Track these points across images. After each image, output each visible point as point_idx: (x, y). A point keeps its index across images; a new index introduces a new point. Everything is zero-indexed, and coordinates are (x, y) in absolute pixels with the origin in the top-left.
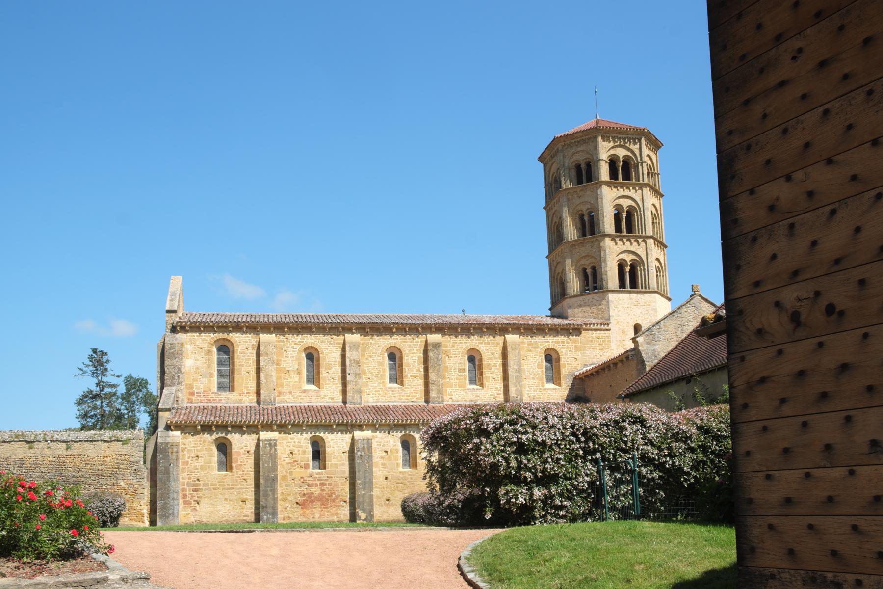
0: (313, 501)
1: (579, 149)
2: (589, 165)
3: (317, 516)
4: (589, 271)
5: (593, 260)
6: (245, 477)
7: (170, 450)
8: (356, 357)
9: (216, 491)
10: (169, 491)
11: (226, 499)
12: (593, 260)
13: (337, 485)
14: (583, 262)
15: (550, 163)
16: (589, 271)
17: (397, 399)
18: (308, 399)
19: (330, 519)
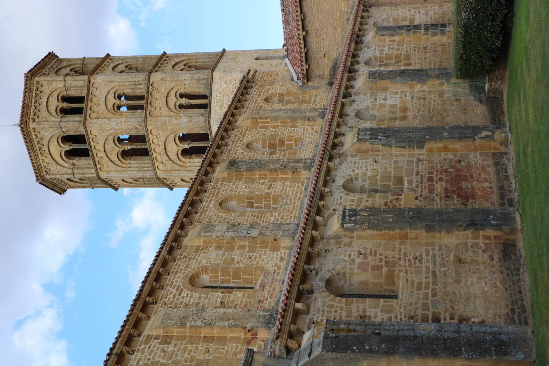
0: (460, 189)
1: (45, 104)
2: (66, 99)
3: (486, 184)
4: (184, 101)
5: (173, 93)
6: (411, 257)
7: (342, 334)
8: (225, 227)
9: (440, 294)
10: (437, 338)
11: (457, 281)
12: (173, 93)
13: (432, 168)
14: (172, 105)
15: (49, 159)
16: (184, 101)
17: (298, 203)
18: (277, 285)
19: (492, 174)
